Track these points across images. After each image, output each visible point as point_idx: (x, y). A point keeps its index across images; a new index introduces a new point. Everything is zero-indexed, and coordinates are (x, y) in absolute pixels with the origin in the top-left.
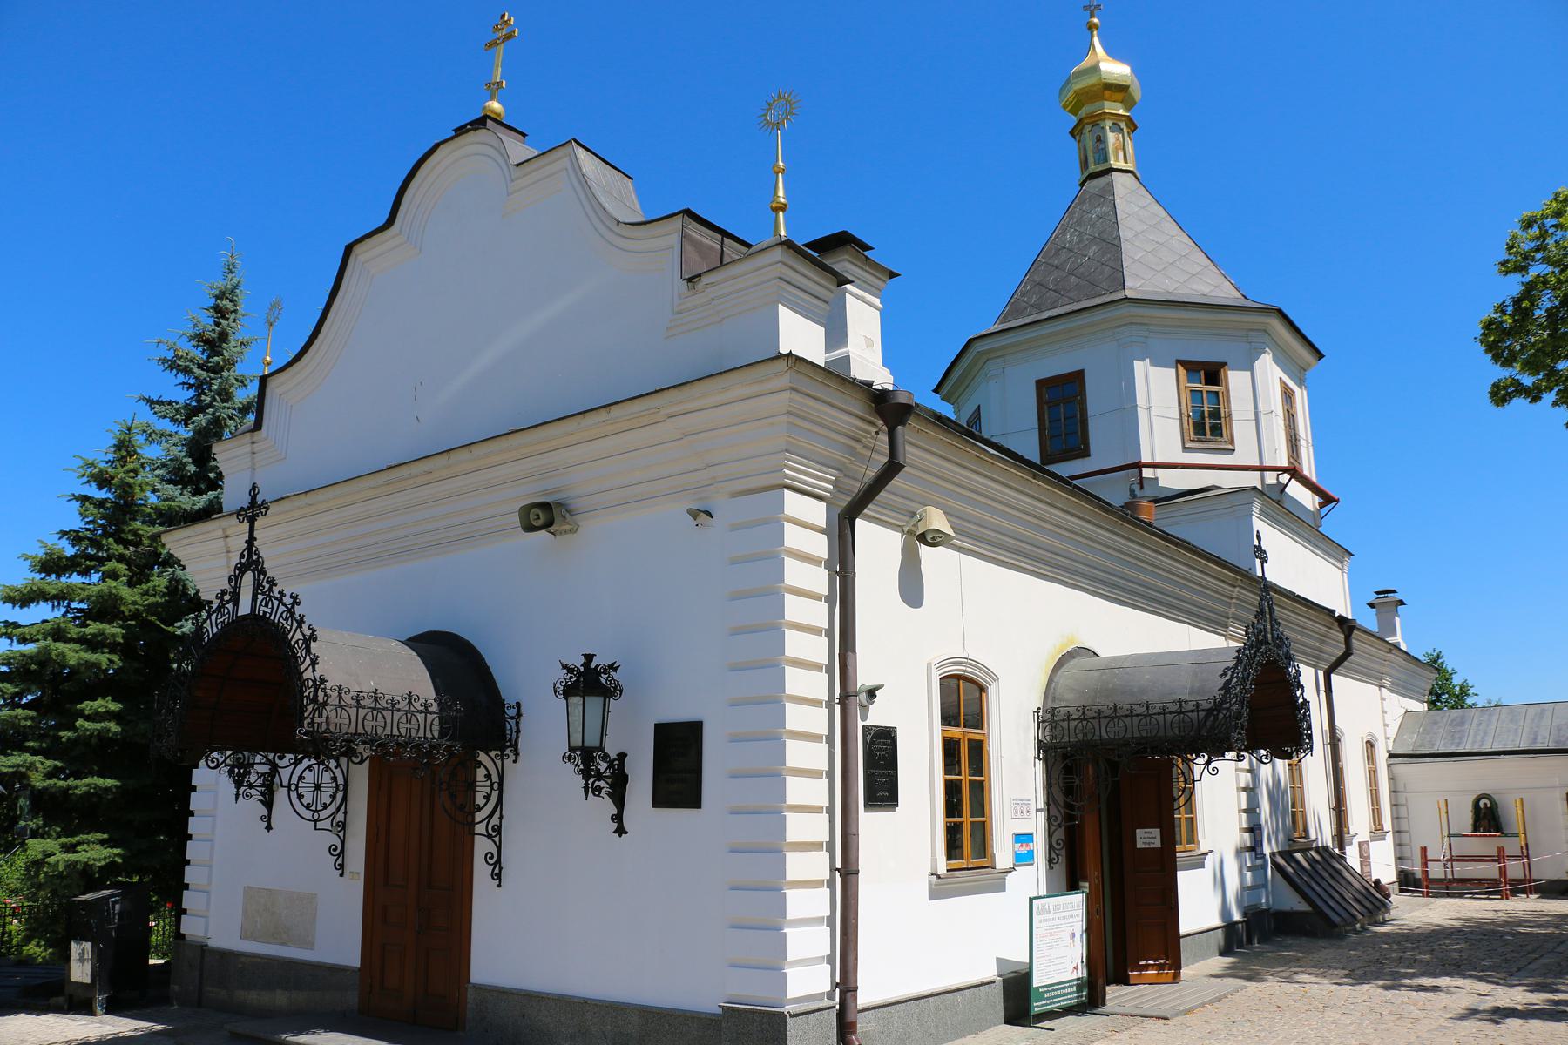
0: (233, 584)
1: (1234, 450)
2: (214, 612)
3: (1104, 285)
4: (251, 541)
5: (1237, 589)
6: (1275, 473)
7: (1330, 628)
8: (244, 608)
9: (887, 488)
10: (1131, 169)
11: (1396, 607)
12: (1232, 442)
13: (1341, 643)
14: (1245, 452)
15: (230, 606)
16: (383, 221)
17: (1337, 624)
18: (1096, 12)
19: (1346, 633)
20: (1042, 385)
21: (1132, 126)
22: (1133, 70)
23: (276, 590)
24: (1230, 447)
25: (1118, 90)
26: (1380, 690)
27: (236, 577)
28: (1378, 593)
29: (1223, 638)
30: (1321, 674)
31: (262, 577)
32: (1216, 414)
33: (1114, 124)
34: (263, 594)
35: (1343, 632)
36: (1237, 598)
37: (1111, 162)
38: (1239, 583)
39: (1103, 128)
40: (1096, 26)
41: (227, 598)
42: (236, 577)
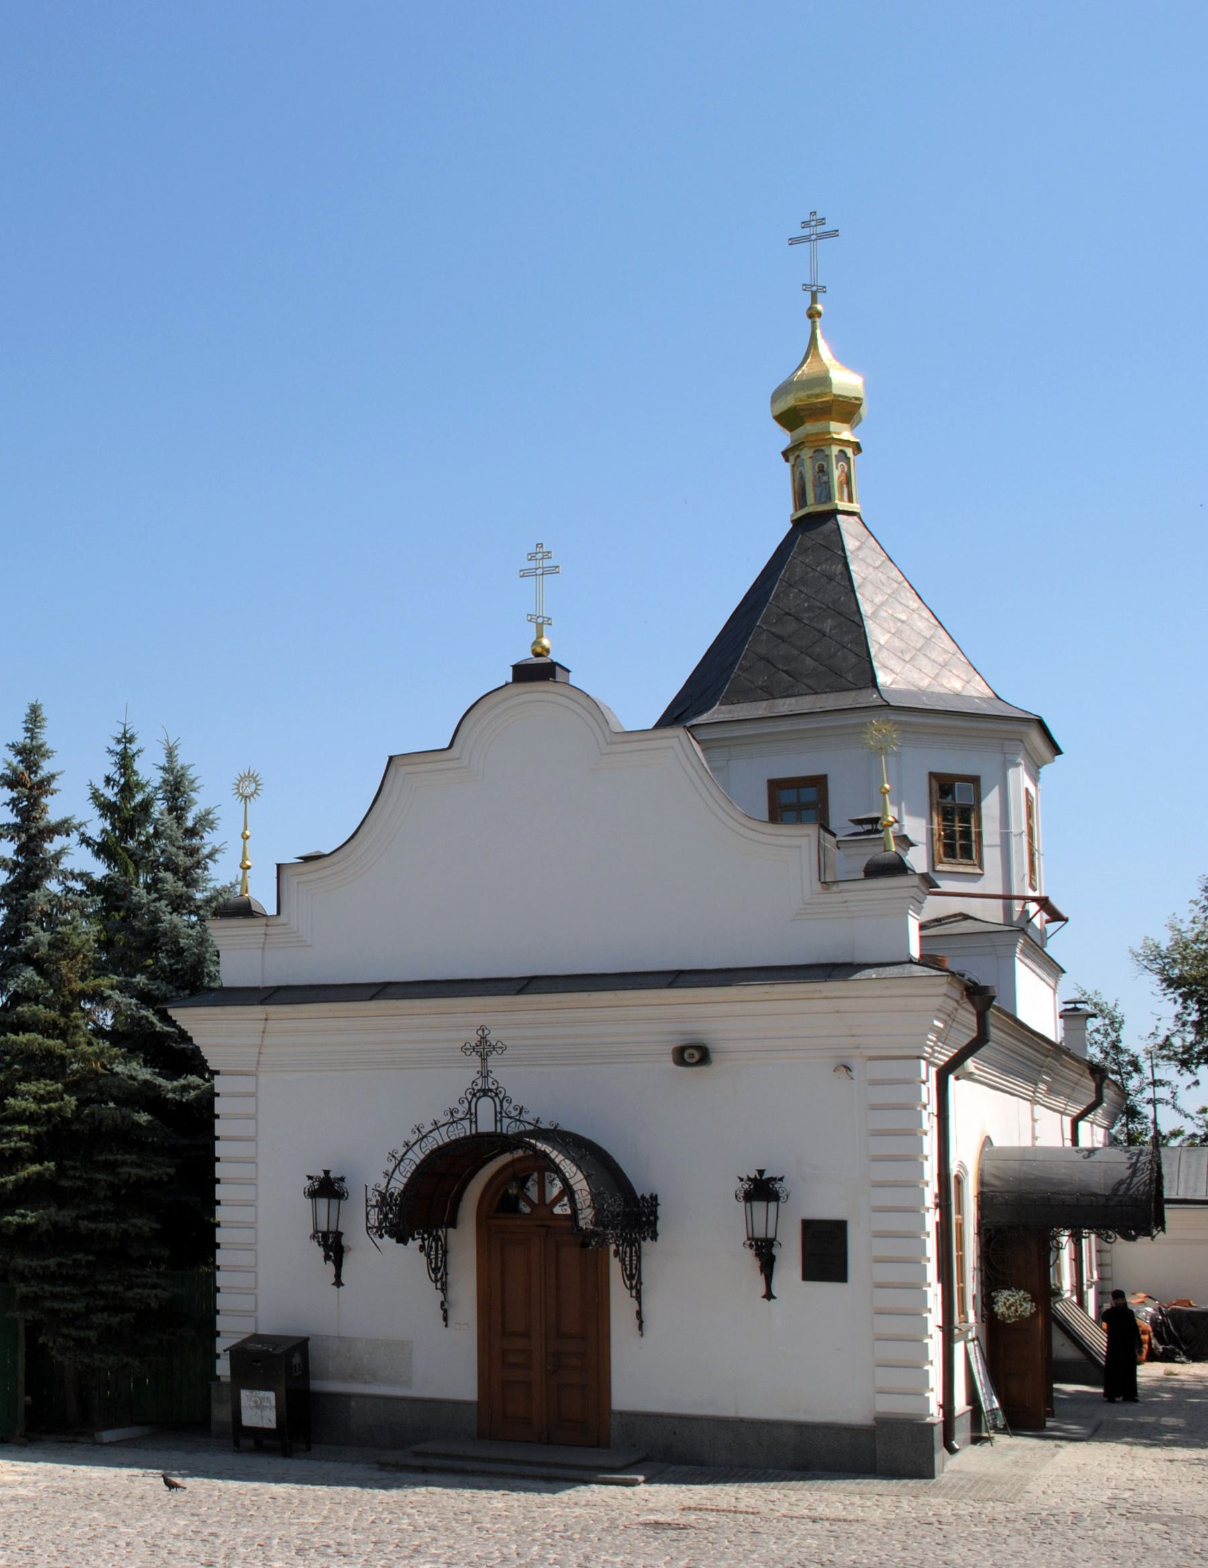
0: (466, 1105)
1: (982, 875)
2: (444, 1125)
3: (850, 677)
4: (485, 1075)
5: (1049, 1059)
6: (1022, 902)
7: (1081, 1076)
8: (486, 1124)
9: (976, 1055)
10: (858, 511)
11: (1087, 1019)
12: (981, 866)
13: (1090, 1091)
14: (992, 882)
15: (466, 1123)
16: (446, 746)
17: (1088, 1071)
18: (819, 295)
19: (1098, 1081)
20: (776, 786)
21: (857, 448)
22: (865, 383)
23: (525, 1117)
24: (978, 871)
25: (848, 410)
26: (1092, 1126)
27: (470, 1103)
28: (1065, 1003)
29: (1028, 1103)
30: (1067, 1121)
31: (505, 1104)
32: (966, 834)
33: (841, 451)
34: (511, 1118)
35: (1094, 1080)
36: (1047, 1067)
37: (837, 501)
38: (1051, 1053)
39: (827, 456)
40: (819, 314)
41: (460, 1115)
42: (470, 1103)
